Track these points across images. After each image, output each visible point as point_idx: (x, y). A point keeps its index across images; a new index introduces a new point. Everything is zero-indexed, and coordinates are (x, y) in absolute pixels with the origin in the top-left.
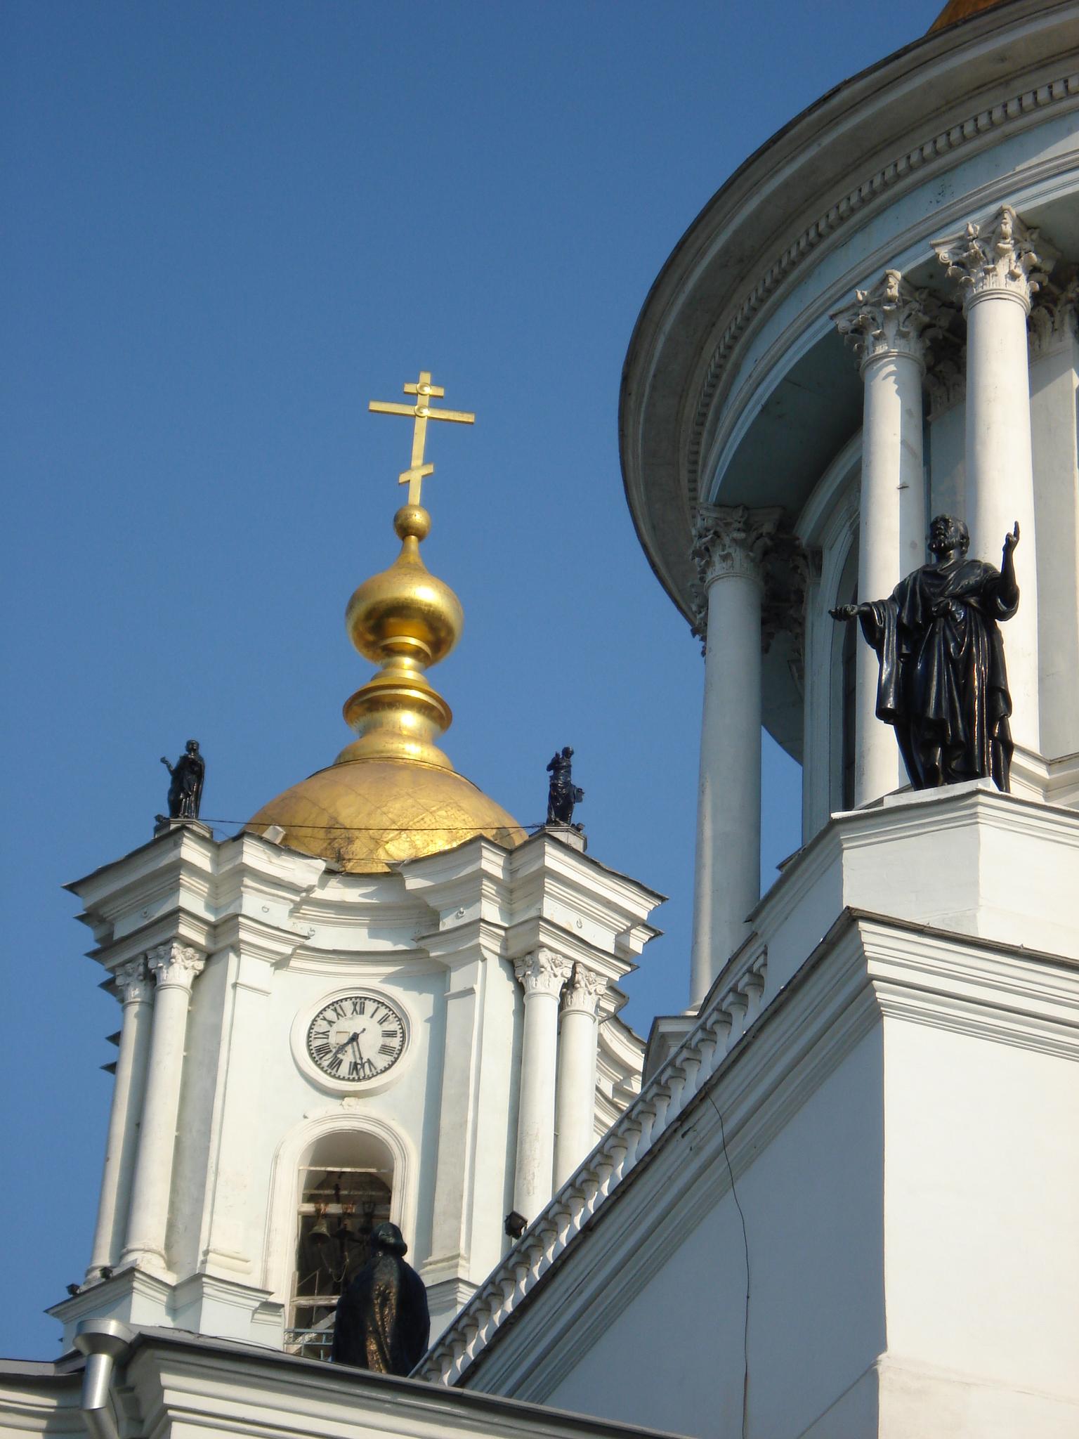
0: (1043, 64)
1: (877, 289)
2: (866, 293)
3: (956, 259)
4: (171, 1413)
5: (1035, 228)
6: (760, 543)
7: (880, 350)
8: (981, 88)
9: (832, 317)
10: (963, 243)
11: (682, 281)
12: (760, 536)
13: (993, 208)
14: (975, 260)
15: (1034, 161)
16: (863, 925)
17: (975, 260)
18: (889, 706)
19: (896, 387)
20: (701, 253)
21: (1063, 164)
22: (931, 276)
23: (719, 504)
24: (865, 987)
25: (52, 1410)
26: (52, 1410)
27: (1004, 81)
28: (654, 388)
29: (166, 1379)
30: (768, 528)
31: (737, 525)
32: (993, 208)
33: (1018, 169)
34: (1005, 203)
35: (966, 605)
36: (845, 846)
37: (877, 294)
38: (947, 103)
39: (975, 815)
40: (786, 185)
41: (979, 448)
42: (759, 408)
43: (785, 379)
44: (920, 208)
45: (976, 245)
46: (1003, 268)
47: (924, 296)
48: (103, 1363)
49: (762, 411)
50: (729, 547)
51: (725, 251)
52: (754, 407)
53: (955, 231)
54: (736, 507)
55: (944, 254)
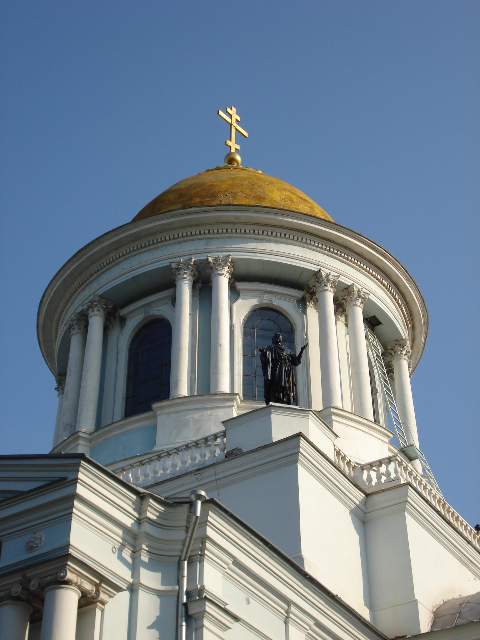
0: (245, 224)
1: (187, 260)
2: (183, 260)
3: (213, 262)
4: (208, 523)
5: (233, 262)
6: (107, 310)
7: (185, 276)
8: (227, 223)
9: (170, 263)
10: (216, 259)
11: (116, 235)
12: (107, 308)
13: (228, 253)
14: (220, 264)
15: (237, 246)
16: (301, 438)
17: (220, 264)
18: (269, 378)
19: (188, 287)
20: (127, 230)
21: (247, 250)
22: (201, 263)
23: (100, 296)
24: (296, 453)
25: (162, 511)
26: (162, 511)
27: (234, 223)
28: (87, 258)
29: (210, 513)
30: (110, 307)
31: (103, 303)
32: (228, 253)
33: (232, 246)
34: (231, 254)
35: (288, 359)
36: (272, 413)
37: (187, 262)
38: (217, 222)
39: (308, 416)
40: (163, 224)
41: (219, 312)
42: (132, 276)
43: (145, 273)
44: (200, 245)
45: (220, 260)
46: (226, 268)
47: (196, 267)
48: (199, 503)
49: (132, 278)
50: (100, 308)
51: (135, 233)
52: (130, 275)
53: (216, 255)
54: (104, 298)
55: (211, 259)
